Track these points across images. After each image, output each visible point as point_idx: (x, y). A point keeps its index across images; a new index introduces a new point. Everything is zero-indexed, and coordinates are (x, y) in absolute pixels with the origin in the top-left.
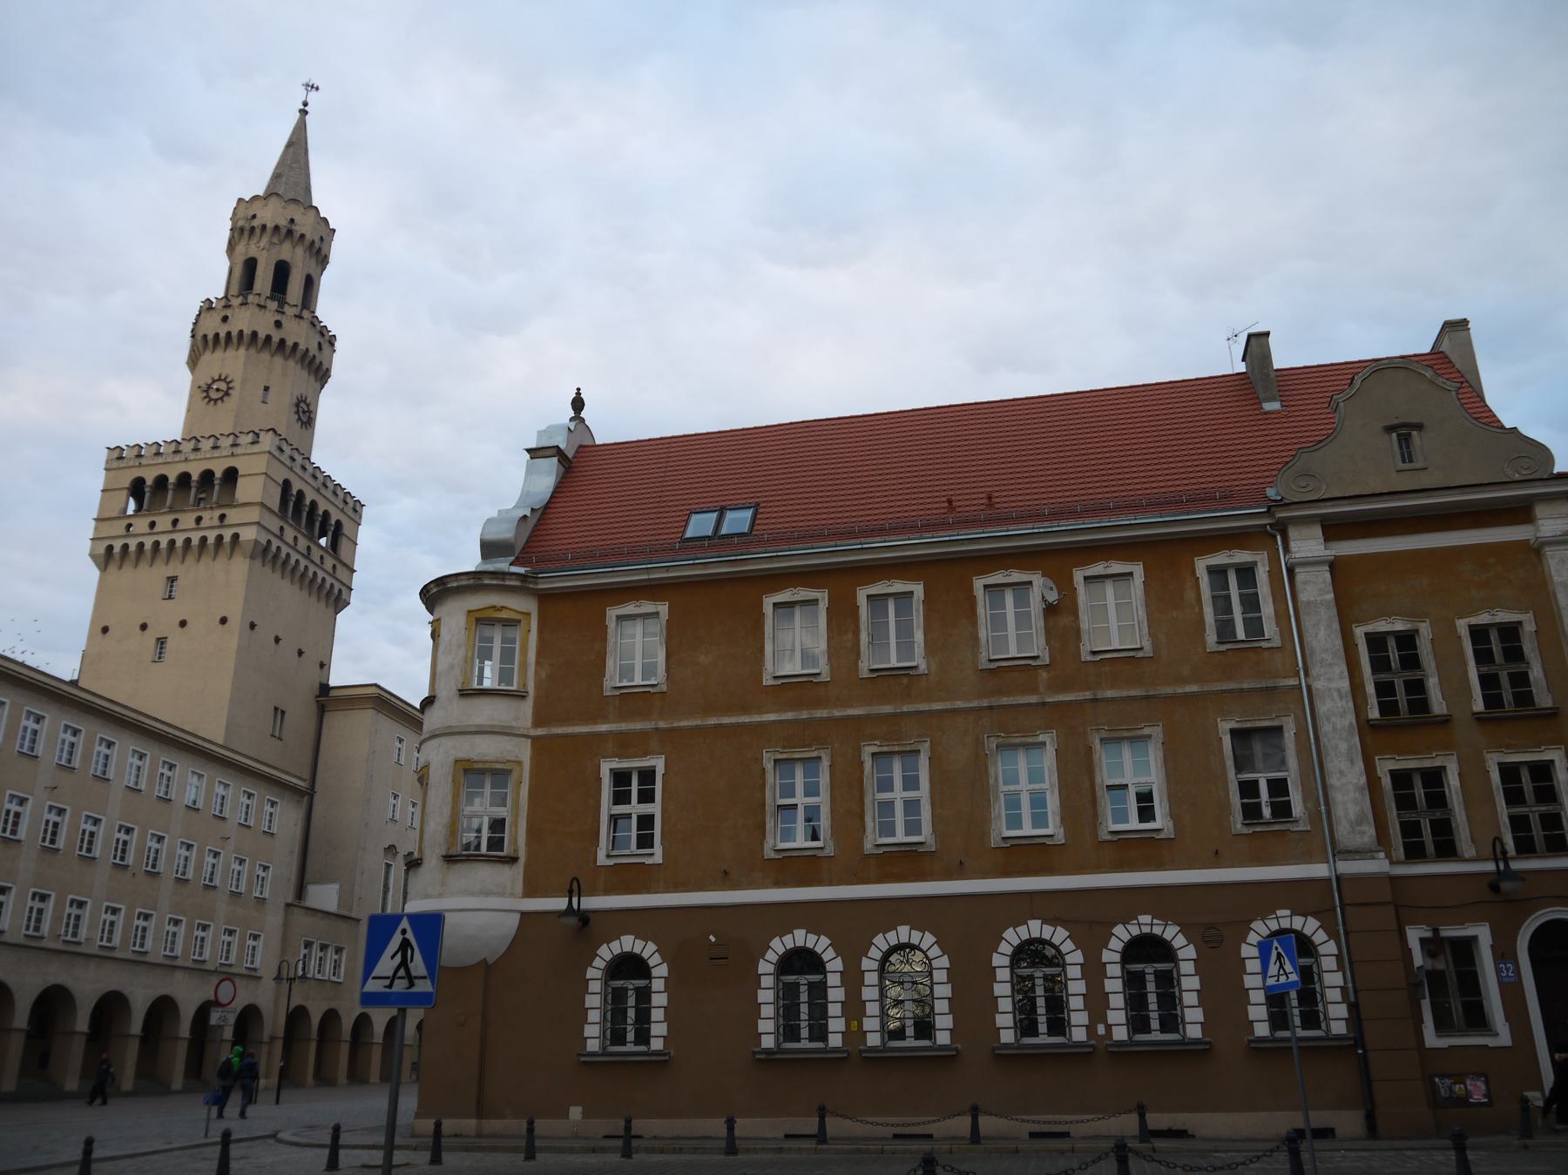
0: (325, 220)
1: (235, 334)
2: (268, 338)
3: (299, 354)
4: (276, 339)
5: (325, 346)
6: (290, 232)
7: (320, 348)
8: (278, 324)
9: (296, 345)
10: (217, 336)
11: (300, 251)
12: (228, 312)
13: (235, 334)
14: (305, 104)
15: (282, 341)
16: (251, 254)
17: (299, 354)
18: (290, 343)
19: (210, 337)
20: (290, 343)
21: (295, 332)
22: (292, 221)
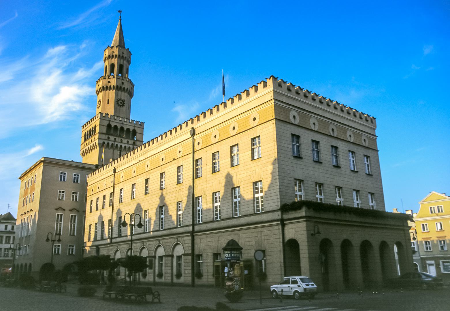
0: (130, 52)
1: (112, 86)
2: (121, 87)
3: (128, 91)
4: (123, 87)
5: (133, 88)
6: (123, 57)
7: (132, 89)
8: (123, 83)
9: (127, 89)
10: (107, 87)
11: (125, 62)
12: (109, 80)
13: (112, 86)
14: (120, 17)
15: (124, 88)
16: (113, 63)
17: (128, 91)
18: (126, 88)
19: (105, 87)
20: (126, 88)
21: (126, 86)
22: (123, 53)
